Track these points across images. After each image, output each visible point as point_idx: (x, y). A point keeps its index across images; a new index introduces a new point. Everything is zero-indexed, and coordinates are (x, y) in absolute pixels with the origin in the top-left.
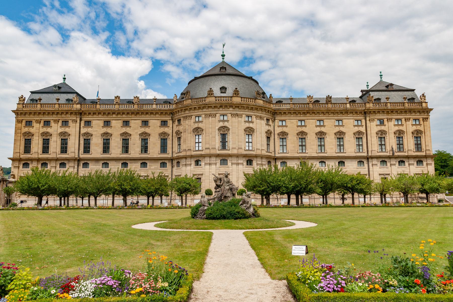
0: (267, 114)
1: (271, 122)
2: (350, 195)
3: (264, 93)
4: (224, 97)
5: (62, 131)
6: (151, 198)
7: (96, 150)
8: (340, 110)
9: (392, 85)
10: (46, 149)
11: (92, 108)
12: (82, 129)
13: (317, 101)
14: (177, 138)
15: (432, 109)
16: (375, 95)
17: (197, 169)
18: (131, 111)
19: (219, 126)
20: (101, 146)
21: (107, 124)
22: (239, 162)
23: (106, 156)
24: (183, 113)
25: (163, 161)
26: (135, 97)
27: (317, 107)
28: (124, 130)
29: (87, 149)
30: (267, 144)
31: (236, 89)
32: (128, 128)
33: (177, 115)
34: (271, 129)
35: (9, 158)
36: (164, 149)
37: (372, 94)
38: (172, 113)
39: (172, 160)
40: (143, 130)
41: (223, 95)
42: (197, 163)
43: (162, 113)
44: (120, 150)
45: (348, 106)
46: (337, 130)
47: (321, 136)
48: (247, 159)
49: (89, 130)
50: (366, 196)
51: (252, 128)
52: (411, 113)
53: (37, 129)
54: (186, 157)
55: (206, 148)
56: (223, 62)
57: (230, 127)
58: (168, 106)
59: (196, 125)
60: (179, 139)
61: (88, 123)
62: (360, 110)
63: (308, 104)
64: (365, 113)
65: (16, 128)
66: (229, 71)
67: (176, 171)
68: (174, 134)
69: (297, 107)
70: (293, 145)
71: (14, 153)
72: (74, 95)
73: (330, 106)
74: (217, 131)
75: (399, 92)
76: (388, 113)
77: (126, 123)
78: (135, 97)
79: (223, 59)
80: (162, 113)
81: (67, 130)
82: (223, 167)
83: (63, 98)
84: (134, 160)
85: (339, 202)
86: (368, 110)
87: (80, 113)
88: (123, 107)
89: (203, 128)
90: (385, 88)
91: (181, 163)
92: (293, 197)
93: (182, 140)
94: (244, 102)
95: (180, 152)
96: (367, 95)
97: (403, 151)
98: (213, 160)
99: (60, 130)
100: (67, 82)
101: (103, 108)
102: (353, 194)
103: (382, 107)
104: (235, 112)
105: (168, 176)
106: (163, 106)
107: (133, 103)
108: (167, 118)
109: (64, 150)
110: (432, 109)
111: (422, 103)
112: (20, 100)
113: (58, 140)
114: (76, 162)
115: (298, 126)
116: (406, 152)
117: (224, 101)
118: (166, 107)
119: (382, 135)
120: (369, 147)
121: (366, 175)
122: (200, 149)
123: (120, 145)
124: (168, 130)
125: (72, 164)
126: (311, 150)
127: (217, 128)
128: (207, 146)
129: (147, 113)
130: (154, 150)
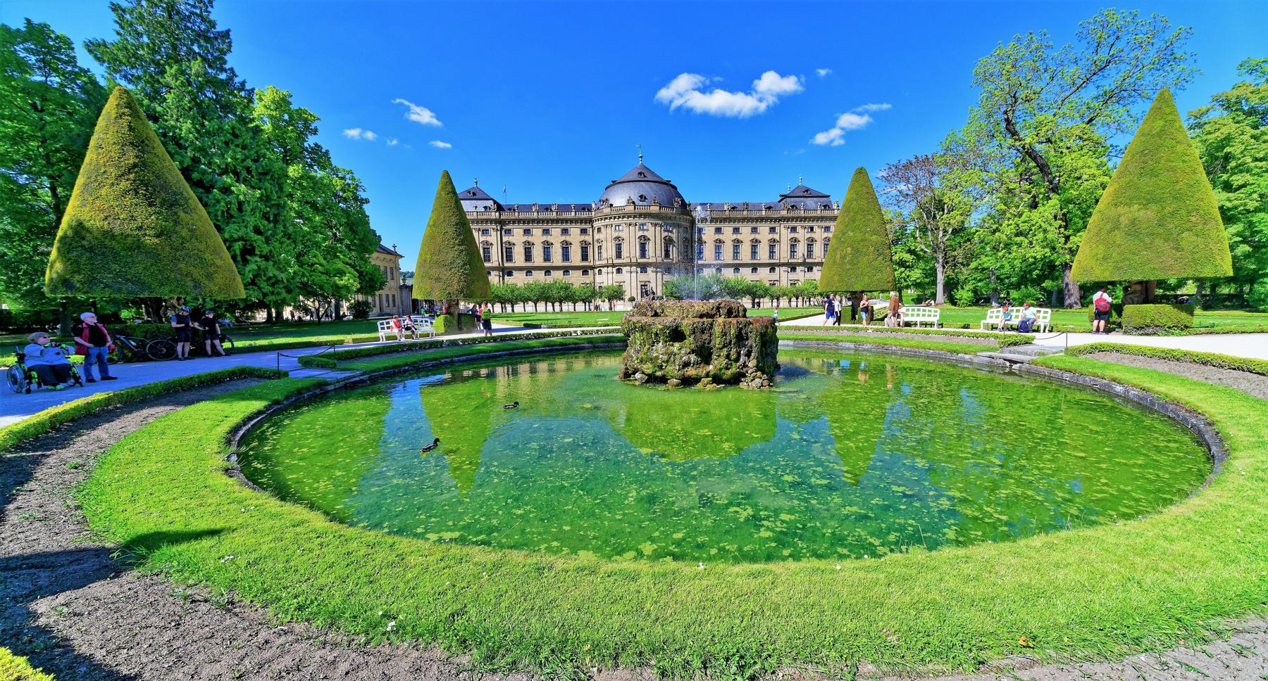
7: (519, 259)
27: (735, 214)
28: (545, 238)
29: (509, 258)
34: (688, 236)
36: (585, 257)
38: (590, 221)
39: (592, 268)
40: (563, 238)
43: (582, 221)
49: (511, 239)
59: (616, 235)
60: (600, 247)
61: (508, 232)
66: (649, 178)
67: (598, 279)
80: (582, 221)
83: (481, 204)
87: (501, 223)
88: (543, 215)
94: (663, 210)
98: (634, 268)
101: (523, 216)
108: (587, 226)
118: (585, 215)
119: (794, 243)
124: (588, 239)
129: (567, 221)
130: (576, 258)
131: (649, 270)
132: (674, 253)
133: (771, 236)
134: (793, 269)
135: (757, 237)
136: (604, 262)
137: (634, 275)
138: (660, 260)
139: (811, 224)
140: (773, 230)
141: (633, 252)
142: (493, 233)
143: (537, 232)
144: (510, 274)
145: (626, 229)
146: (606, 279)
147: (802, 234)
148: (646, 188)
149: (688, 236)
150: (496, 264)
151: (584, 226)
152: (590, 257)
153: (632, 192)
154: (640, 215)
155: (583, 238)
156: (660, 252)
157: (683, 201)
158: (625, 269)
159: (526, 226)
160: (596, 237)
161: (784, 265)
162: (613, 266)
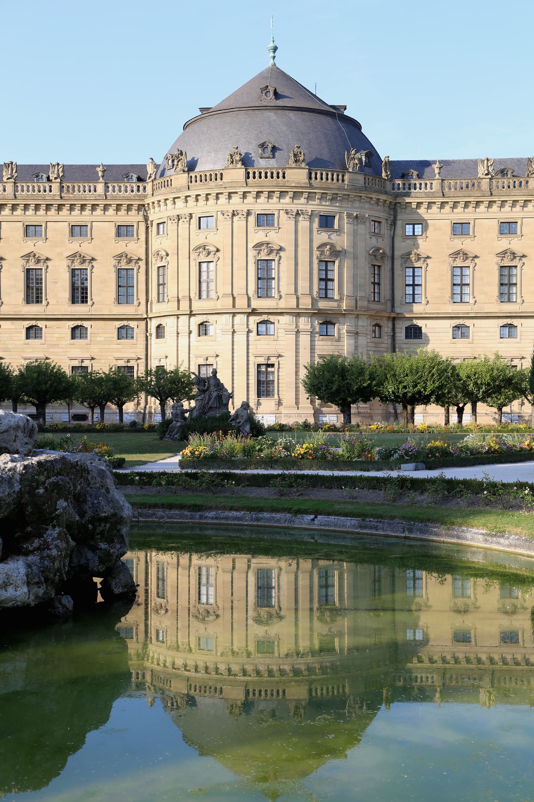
0: (375, 207)
30: (374, 283)
34: (384, 245)
40: (74, 246)
44: (22, 295)
55: (225, 295)
107: (48, 179)
108: (133, 218)
124: (135, 248)
127: (250, 245)
137: (240, 338)
151: (123, 218)
157: (372, 153)
160: (156, 244)
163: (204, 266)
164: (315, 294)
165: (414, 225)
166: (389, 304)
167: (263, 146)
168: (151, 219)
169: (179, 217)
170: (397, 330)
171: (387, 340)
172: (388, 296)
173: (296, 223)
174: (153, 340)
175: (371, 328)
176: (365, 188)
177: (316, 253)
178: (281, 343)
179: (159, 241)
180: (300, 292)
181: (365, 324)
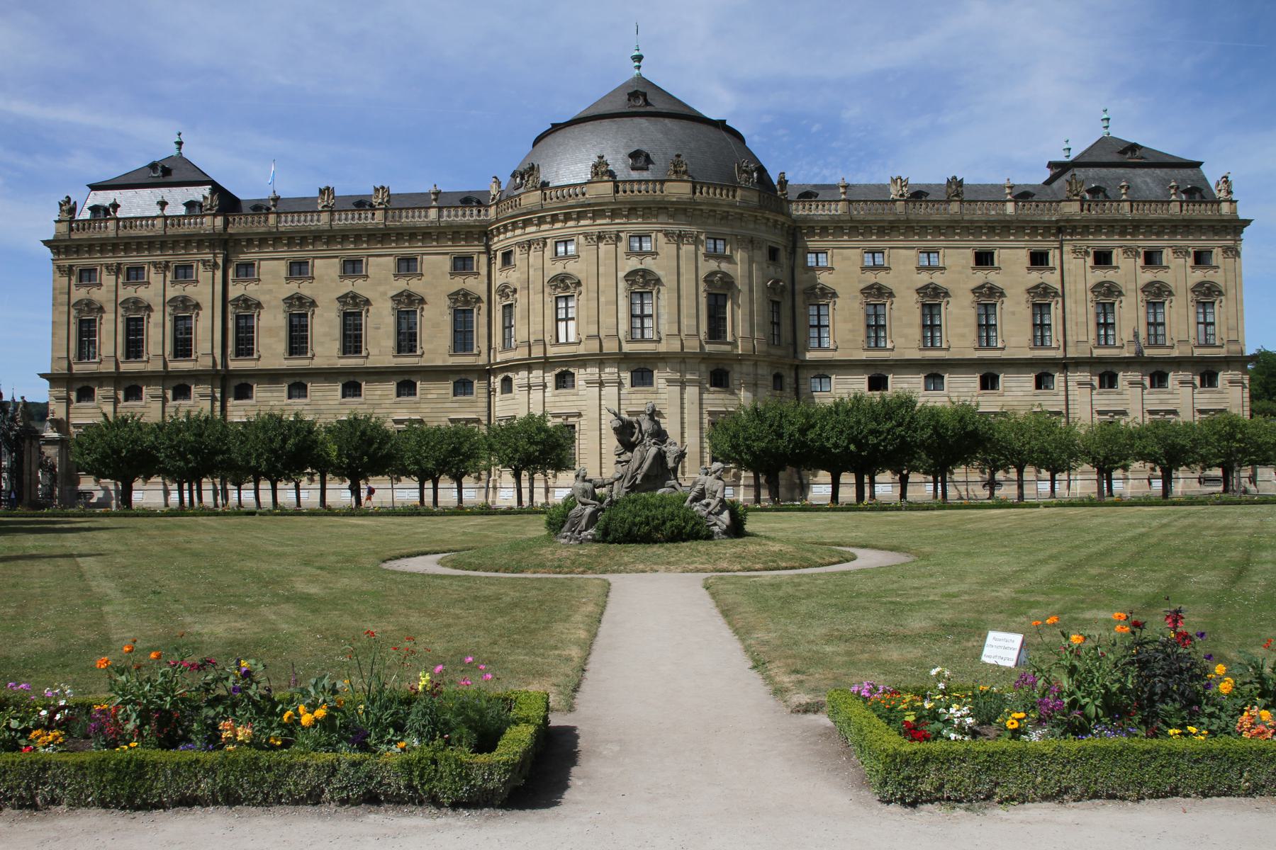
1: (783, 256)
2: (1013, 474)
3: (761, 170)
4: (640, 181)
5: (177, 294)
6: (429, 485)
7: (271, 350)
8: (987, 222)
9: (1134, 147)
10: (134, 347)
11: (259, 226)
12: (231, 287)
13: (918, 195)
14: (499, 308)
15: (1247, 222)
16: (1091, 176)
17: (562, 398)
18: (366, 230)
19: (628, 270)
20: (283, 334)
21: (298, 269)
22: (688, 377)
23: (298, 363)
24: (518, 232)
25: (463, 376)
26: (377, 190)
28: (347, 286)
29: (245, 345)
30: (773, 323)
31: (678, 156)
32: (360, 281)
33: (502, 237)
35: (43, 376)
36: (462, 339)
37: (1080, 173)
38: (484, 234)
39: (486, 373)
40: (401, 285)
41: (635, 175)
42: (564, 380)
45: (1010, 208)
46: (980, 282)
47: (932, 300)
48: (713, 368)
49: (251, 290)
50: (1057, 477)
51: (725, 274)
52: (1189, 233)
53: (106, 290)
54: (529, 367)
55: (589, 337)
56: (640, 79)
57: (660, 273)
58: (475, 212)
59: (558, 268)
60: (508, 308)
61: (246, 271)
62: (1045, 222)
63: (894, 201)
64: (1061, 229)
65: (54, 289)
68: (496, 297)
69: (860, 212)
70: (849, 326)
71: (55, 360)
72: (206, 190)
73: (954, 207)
74: (622, 285)
75: (1158, 171)
76: (1123, 233)
77: (352, 268)
78: (377, 190)
79: (639, 67)
81: (190, 291)
82: (642, 392)
83: (177, 199)
84: (379, 374)
85: (983, 493)
86: (1067, 221)
88: (344, 221)
89: (581, 276)
90: (1116, 158)
91: (514, 382)
92: (848, 478)
93: (518, 312)
94: (704, 195)
95: (510, 349)
96: (1067, 176)
97: (1163, 346)
98: (610, 372)
99: (172, 292)
100: (186, 152)
101: (288, 223)
102: (1020, 472)
103: (1109, 211)
104: (675, 228)
105: (478, 421)
106: (460, 213)
107: (371, 205)
108: (474, 249)
109: (183, 347)
110: (1247, 222)
111: (1219, 202)
112: (62, 211)
113: (168, 318)
114: (219, 384)
115: (864, 269)
116: (1172, 347)
117: (641, 194)
118: (470, 217)
119: (1107, 295)
120: (1068, 333)
121: (1058, 413)
122: (571, 339)
123: (337, 332)
124: (475, 285)
125: (206, 389)
126: (903, 340)
127: (621, 274)
128: (593, 330)
129: (412, 234)
130: (435, 345)
131: (660, 377)
132: (738, 321)
133: (1035, 277)
134: (1108, 380)
135: (993, 278)
136: (521, 354)
138: (692, 346)
139: (1153, 243)
140: (1039, 259)
141: (607, 321)
142: (203, 274)
143: (326, 268)
144: (243, 392)
145: (588, 253)
146: (520, 402)
147: (1128, 272)
148: (646, 134)
149: (783, 274)
150: (204, 363)
152: (480, 342)
153: (611, 145)
154: (633, 210)
155: (458, 283)
156: (695, 322)
158: (581, 375)
159: (297, 254)
160: (499, 278)
161: (1078, 364)
162: (546, 363)
163: (562, 304)
164: (702, 337)
165: (817, 254)
166: (791, 350)
167: (635, 155)
168: (494, 248)
169: (530, 243)
170: (801, 381)
171: (788, 391)
172: (790, 340)
173: (678, 248)
174: (498, 398)
175: (771, 378)
176: (762, 207)
177: (702, 286)
178: (663, 396)
179: (504, 274)
180: (685, 331)
181: (765, 371)
